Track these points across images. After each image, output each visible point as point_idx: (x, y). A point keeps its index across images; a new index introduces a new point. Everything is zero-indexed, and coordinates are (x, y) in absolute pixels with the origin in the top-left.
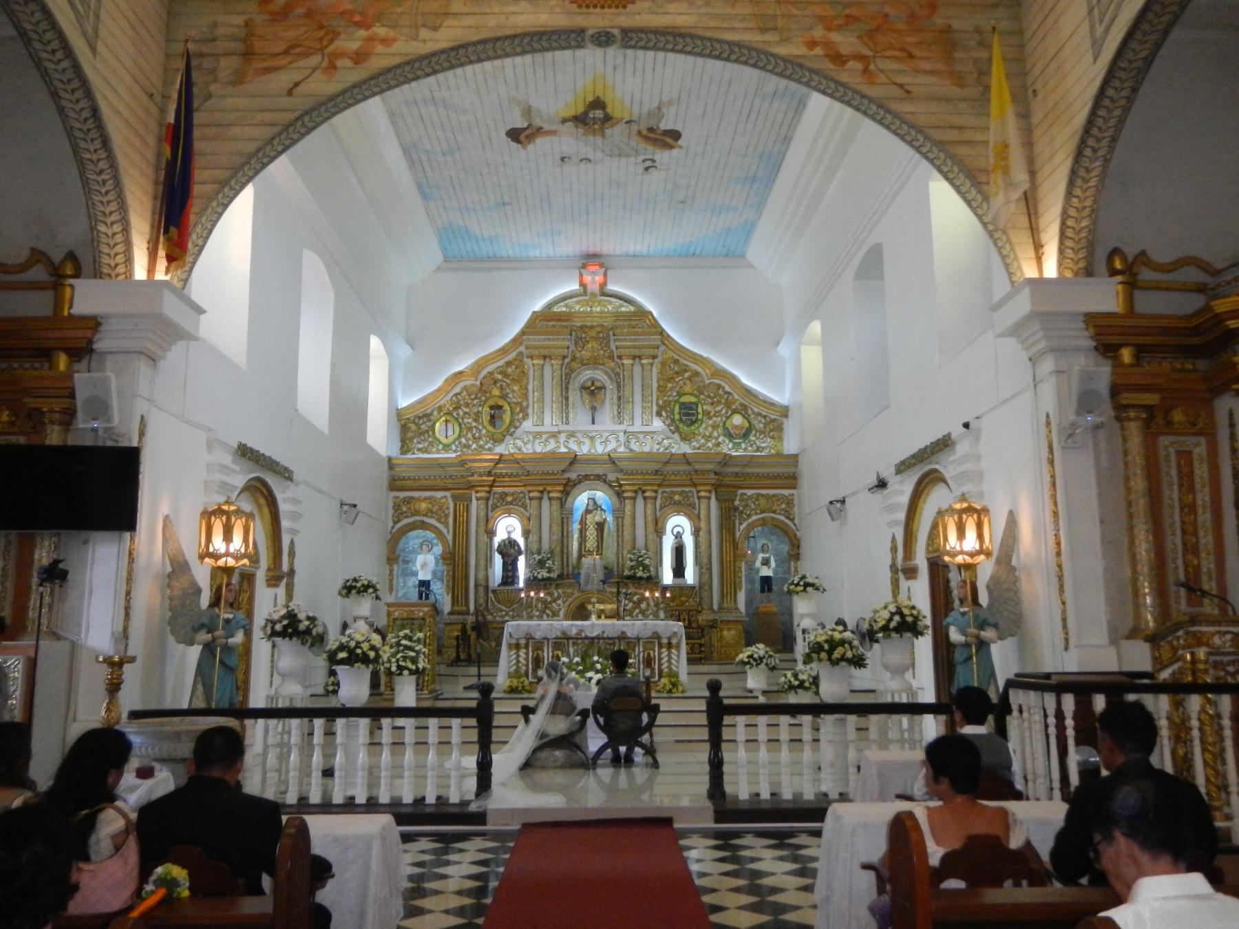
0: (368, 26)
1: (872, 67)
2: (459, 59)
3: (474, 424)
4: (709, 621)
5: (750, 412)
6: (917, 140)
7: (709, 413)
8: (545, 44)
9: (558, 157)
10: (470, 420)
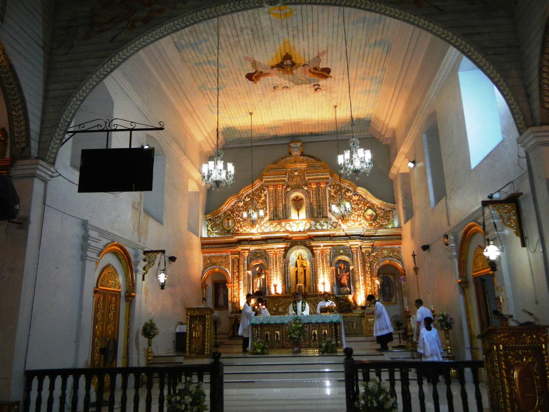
2: (198, 18)
3: (241, 220)
4: (361, 314)
5: (376, 208)
6: (449, 36)
7: (355, 209)
8: (242, 6)
9: (272, 86)
10: (239, 218)
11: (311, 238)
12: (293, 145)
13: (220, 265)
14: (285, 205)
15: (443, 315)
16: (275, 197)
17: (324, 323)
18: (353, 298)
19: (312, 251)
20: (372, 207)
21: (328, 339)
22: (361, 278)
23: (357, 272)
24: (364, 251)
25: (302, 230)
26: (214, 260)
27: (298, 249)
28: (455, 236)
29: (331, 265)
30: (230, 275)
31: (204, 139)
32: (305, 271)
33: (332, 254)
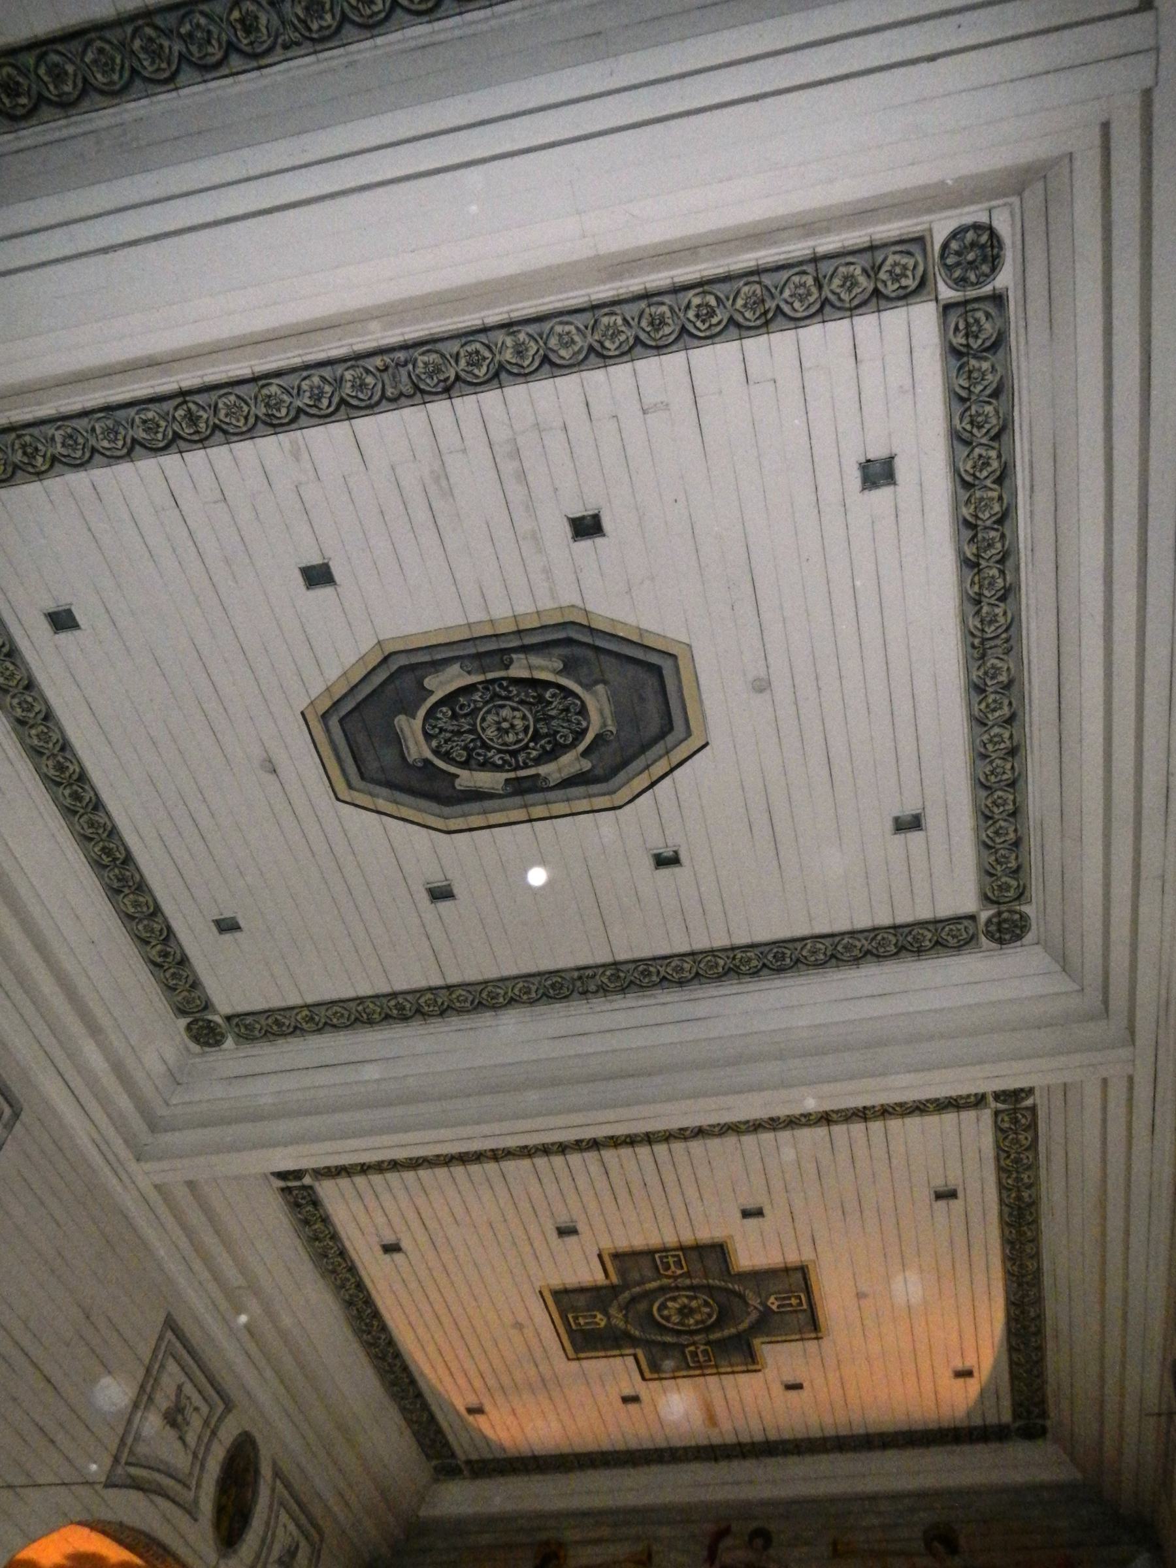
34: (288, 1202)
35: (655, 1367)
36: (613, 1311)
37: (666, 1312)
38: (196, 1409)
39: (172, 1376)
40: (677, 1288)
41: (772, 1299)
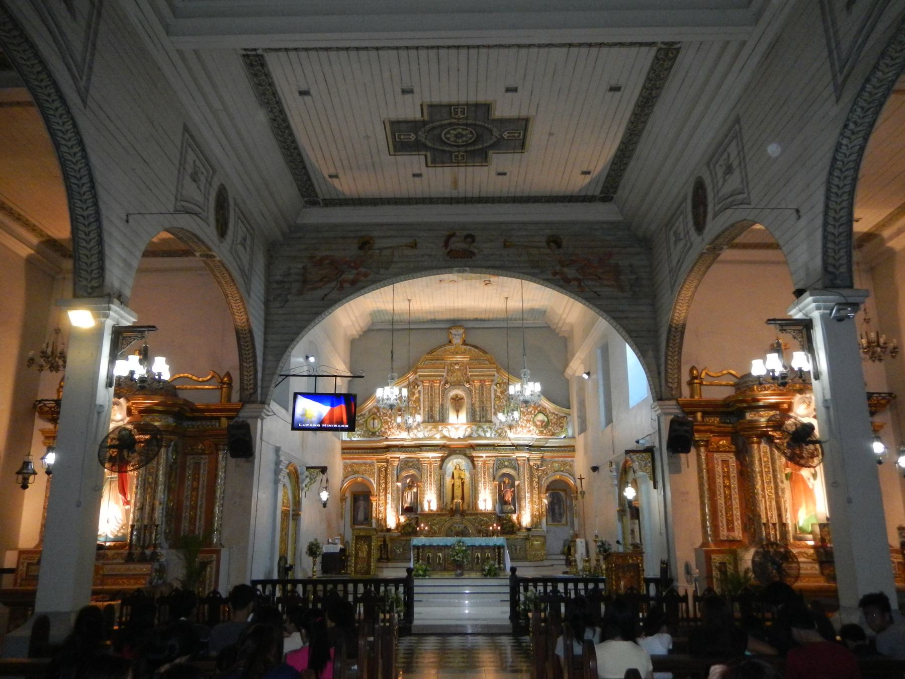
0: (356, 269)
1: (582, 284)
3: (389, 420)
7: (524, 413)
11: (473, 447)
12: (453, 331)
13: (363, 474)
14: (442, 405)
15: (602, 542)
16: (431, 395)
17: (488, 547)
18: (518, 518)
19: (473, 462)
20: (543, 411)
21: (492, 562)
22: (528, 495)
23: (523, 488)
24: (532, 463)
25: (462, 437)
26: (356, 468)
27: (457, 458)
28: (617, 464)
29: (494, 479)
30: (375, 486)
31: (350, 323)
32: (463, 484)
33: (495, 466)
34: (246, 63)
35: (434, 161)
36: (420, 133)
37: (448, 136)
38: (202, 173)
39: (191, 157)
40: (458, 124)
41: (506, 133)
